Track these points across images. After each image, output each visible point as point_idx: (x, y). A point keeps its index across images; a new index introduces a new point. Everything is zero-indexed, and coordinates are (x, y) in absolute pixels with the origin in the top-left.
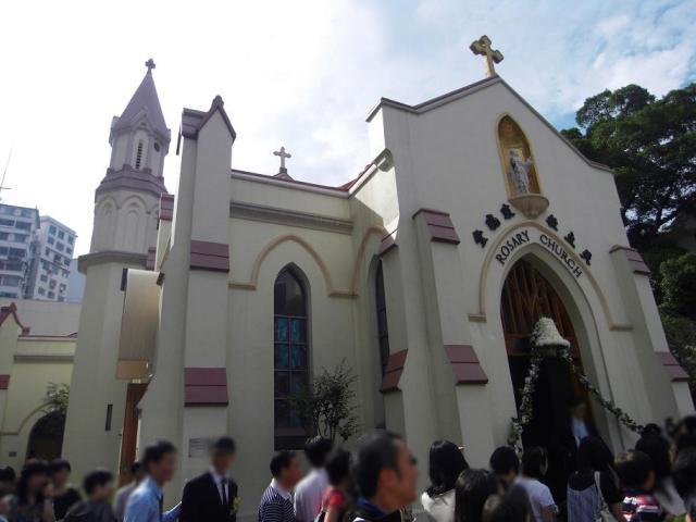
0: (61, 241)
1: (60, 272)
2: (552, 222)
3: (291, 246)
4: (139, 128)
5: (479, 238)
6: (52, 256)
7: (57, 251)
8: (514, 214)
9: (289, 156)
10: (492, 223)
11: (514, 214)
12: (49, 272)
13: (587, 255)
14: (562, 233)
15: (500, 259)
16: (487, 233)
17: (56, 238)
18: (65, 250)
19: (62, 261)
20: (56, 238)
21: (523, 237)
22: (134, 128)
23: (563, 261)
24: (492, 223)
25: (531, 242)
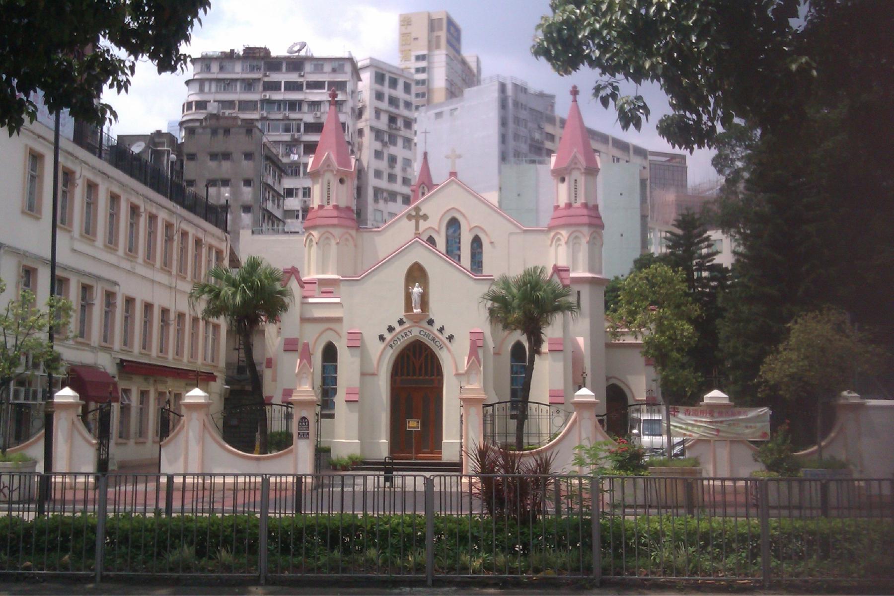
0: (394, 93)
1: (400, 142)
2: (431, 322)
3: (330, 333)
4: (327, 171)
5: (382, 338)
6: (384, 118)
7: (392, 109)
8: (405, 322)
9: (459, 157)
10: (391, 329)
11: (405, 322)
12: (385, 144)
13: (451, 338)
14: (437, 325)
15: (391, 346)
16: (388, 336)
17: (387, 90)
18: (402, 104)
19: (400, 123)
20: (387, 90)
21: (408, 333)
22: (322, 173)
23: (432, 342)
24: (391, 329)
25: (413, 335)
